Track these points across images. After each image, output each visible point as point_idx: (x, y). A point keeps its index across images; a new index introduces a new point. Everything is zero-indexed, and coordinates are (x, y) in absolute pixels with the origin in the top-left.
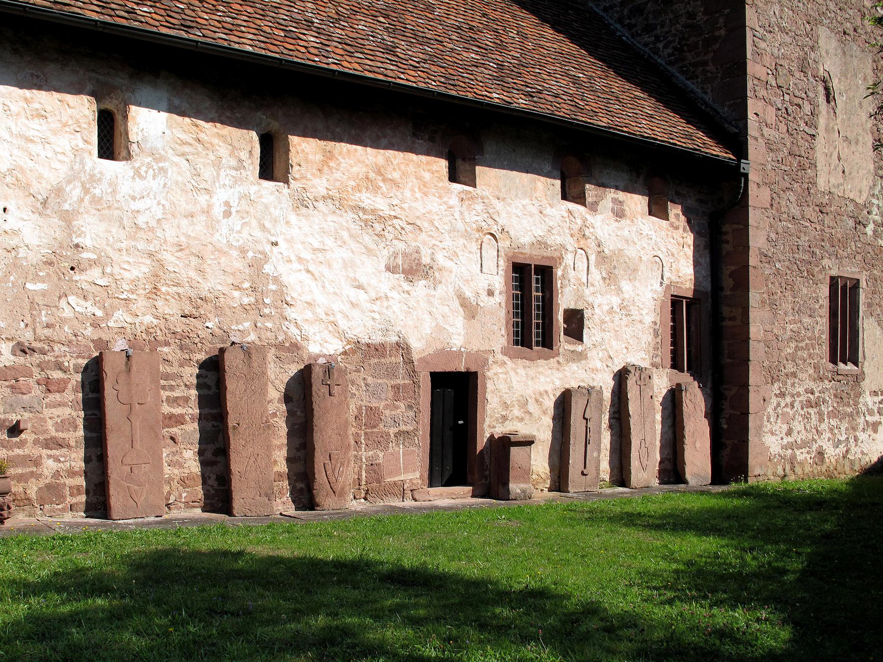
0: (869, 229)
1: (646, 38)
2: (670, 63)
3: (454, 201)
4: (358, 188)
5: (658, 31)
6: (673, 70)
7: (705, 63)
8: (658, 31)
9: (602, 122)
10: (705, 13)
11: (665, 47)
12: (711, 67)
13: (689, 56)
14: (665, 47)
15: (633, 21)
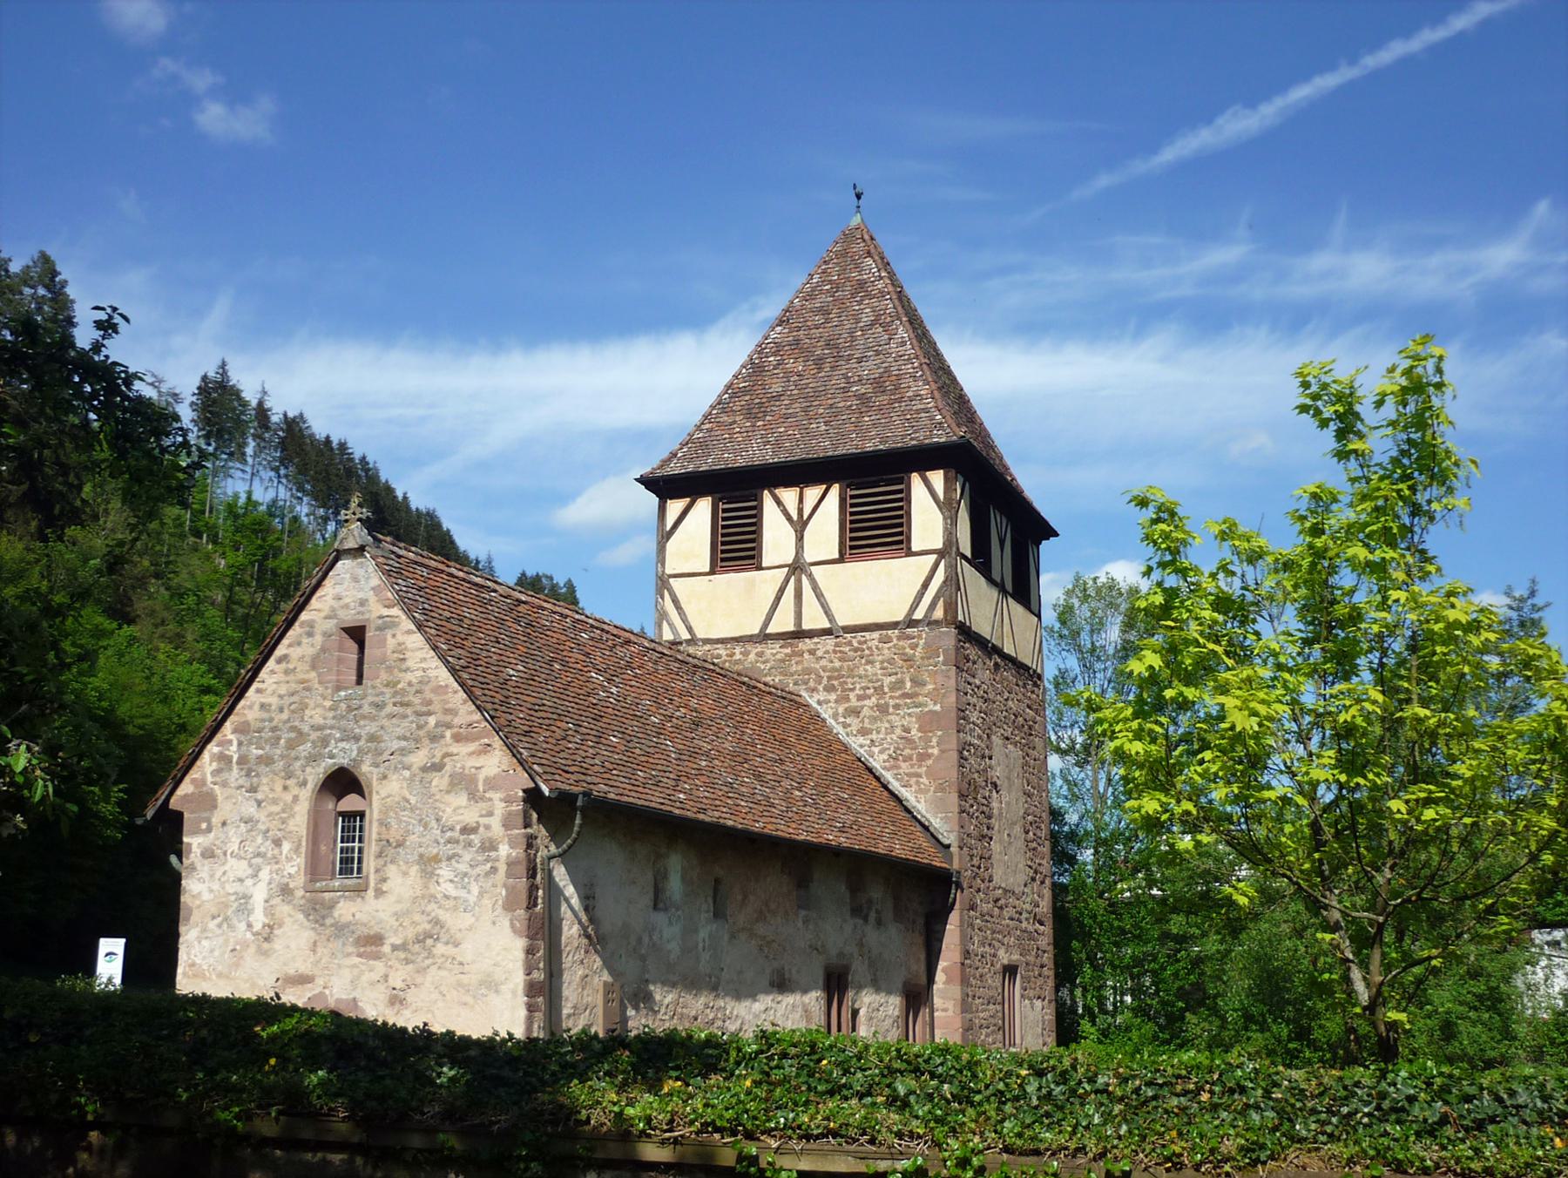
0: (1025, 915)
1: (861, 740)
2: (884, 768)
3: (800, 924)
4: (757, 920)
5: (874, 736)
6: (888, 776)
7: (919, 776)
8: (874, 736)
9: (881, 849)
10: (919, 730)
11: (881, 752)
12: (924, 780)
13: (903, 765)
14: (881, 752)
15: (848, 721)
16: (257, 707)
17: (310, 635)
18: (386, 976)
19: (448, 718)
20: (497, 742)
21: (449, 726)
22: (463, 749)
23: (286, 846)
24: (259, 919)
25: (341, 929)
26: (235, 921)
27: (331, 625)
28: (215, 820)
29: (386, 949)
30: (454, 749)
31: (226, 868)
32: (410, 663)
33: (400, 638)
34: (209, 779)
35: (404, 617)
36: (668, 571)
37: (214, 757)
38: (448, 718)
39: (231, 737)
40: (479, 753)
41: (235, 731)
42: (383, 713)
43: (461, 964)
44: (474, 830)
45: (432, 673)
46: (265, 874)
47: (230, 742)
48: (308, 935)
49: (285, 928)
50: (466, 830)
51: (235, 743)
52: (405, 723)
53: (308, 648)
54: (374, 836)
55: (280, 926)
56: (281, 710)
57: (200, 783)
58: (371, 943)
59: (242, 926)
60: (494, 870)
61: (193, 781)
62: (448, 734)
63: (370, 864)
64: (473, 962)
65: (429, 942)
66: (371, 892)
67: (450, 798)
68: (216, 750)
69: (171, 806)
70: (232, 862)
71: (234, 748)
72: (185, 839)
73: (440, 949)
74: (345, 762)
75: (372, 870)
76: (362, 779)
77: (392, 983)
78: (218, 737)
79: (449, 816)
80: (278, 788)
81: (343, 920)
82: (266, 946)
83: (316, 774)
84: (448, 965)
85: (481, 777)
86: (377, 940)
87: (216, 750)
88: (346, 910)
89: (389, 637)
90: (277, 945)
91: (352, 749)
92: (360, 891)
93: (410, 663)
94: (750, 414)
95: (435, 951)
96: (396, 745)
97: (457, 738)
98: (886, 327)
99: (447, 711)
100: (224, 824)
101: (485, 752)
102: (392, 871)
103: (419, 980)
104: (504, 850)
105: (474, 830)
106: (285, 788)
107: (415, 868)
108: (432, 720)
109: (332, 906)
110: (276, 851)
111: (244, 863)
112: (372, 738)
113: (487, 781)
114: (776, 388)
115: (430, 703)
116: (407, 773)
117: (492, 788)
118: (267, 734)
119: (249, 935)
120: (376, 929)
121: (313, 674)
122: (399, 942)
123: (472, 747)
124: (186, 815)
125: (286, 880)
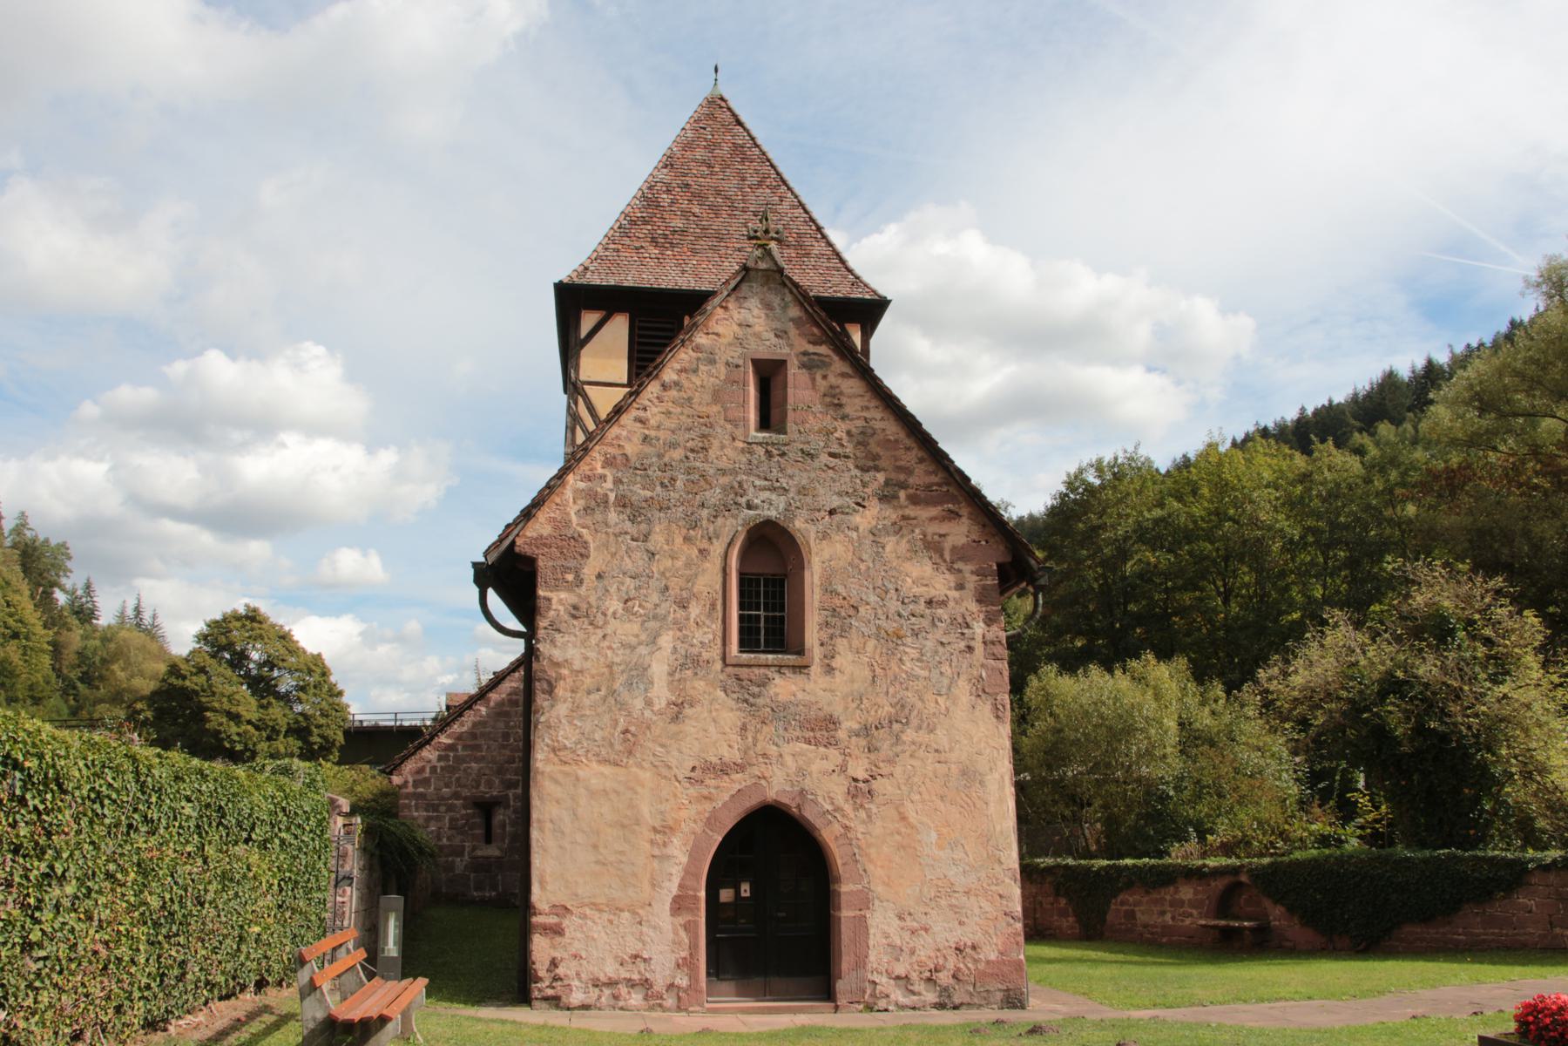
16: (637, 439)
17: (712, 362)
18: (843, 769)
19: (902, 477)
20: (964, 511)
21: (903, 486)
22: (924, 513)
23: (695, 610)
24: (661, 694)
25: (780, 712)
26: (625, 696)
27: (734, 355)
28: (589, 572)
29: (841, 734)
30: (911, 511)
31: (609, 630)
32: (847, 410)
33: (832, 380)
34: (574, 518)
35: (836, 358)
36: (583, 377)
37: (576, 491)
38: (902, 477)
39: (600, 471)
40: (943, 519)
41: (609, 462)
42: (816, 463)
43: (937, 751)
44: (943, 603)
45: (878, 425)
46: (666, 640)
47: (603, 478)
48: (729, 715)
49: (698, 708)
50: (930, 603)
51: (610, 479)
52: (846, 477)
53: (711, 377)
54: (816, 604)
55: (692, 706)
56: (673, 445)
57: (561, 524)
58: (822, 728)
59: (638, 703)
60: (970, 649)
61: (552, 520)
62: (902, 494)
63: (813, 635)
64: (951, 750)
65: (896, 726)
66: (816, 669)
67: (908, 567)
68: (582, 485)
69: (517, 549)
70: (613, 625)
71: (609, 484)
72: (541, 593)
73: (909, 735)
74: (773, 514)
75: (816, 643)
76: (798, 536)
77: (851, 772)
78: (584, 467)
79: (910, 588)
80: (679, 540)
81: (780, 698)
82: (673, 728)
83: (734, 527)
84: (921, 753)
85: (948, 544)
86: (831, 722)
87: (582, 485)
88: (784, 687)
89: (818, 378)
90: (689, 727)
91: (781, 501)
92: (801, 669)
93: (847, 410)
94: (654, 241)
95: (904, 738)
96: (836, 502)
97: (914, 500)
98: (774, 189)
99: (900, 469)
100: (599, 576)
101: (950, 520)
102: (841, 644)
103: (885, 769)
104: (979, 628)
105: (943, 603)
106: (687, 539)
107: (872, 643)
108: (881, 477)
109: (764, 683)
110: (681, 613)
111: (635, 627)
112: (802, 491)
113: (954, 549)
114: (678, 223)
115: (876, 457)
116: (855, 535)
117: (961, 559)
118: (654, 473)
119: (647, 713)
120: (828, 710)
121: (715, 409)
122: (856, 726)
123: (934, 511)
124: (540, 563)
125: (695, 651)
